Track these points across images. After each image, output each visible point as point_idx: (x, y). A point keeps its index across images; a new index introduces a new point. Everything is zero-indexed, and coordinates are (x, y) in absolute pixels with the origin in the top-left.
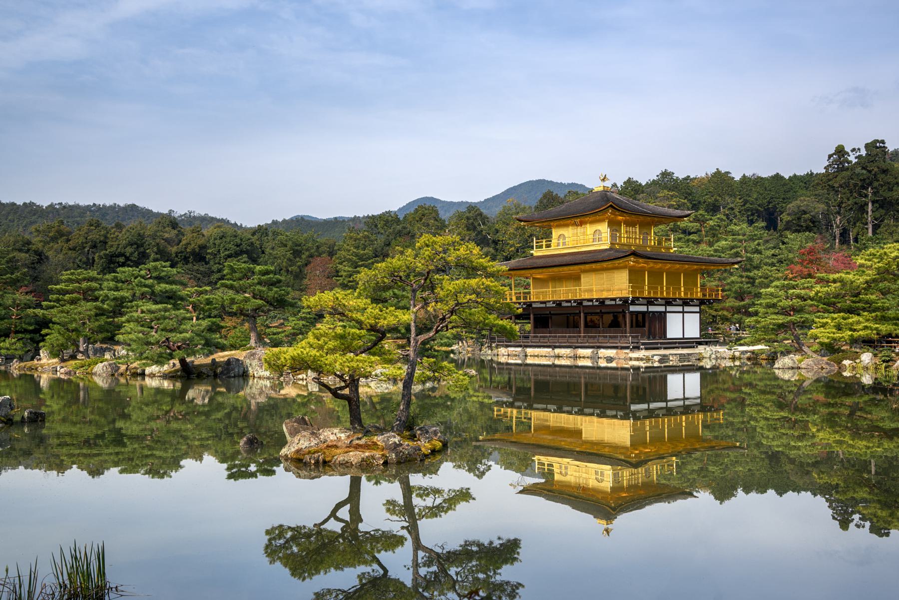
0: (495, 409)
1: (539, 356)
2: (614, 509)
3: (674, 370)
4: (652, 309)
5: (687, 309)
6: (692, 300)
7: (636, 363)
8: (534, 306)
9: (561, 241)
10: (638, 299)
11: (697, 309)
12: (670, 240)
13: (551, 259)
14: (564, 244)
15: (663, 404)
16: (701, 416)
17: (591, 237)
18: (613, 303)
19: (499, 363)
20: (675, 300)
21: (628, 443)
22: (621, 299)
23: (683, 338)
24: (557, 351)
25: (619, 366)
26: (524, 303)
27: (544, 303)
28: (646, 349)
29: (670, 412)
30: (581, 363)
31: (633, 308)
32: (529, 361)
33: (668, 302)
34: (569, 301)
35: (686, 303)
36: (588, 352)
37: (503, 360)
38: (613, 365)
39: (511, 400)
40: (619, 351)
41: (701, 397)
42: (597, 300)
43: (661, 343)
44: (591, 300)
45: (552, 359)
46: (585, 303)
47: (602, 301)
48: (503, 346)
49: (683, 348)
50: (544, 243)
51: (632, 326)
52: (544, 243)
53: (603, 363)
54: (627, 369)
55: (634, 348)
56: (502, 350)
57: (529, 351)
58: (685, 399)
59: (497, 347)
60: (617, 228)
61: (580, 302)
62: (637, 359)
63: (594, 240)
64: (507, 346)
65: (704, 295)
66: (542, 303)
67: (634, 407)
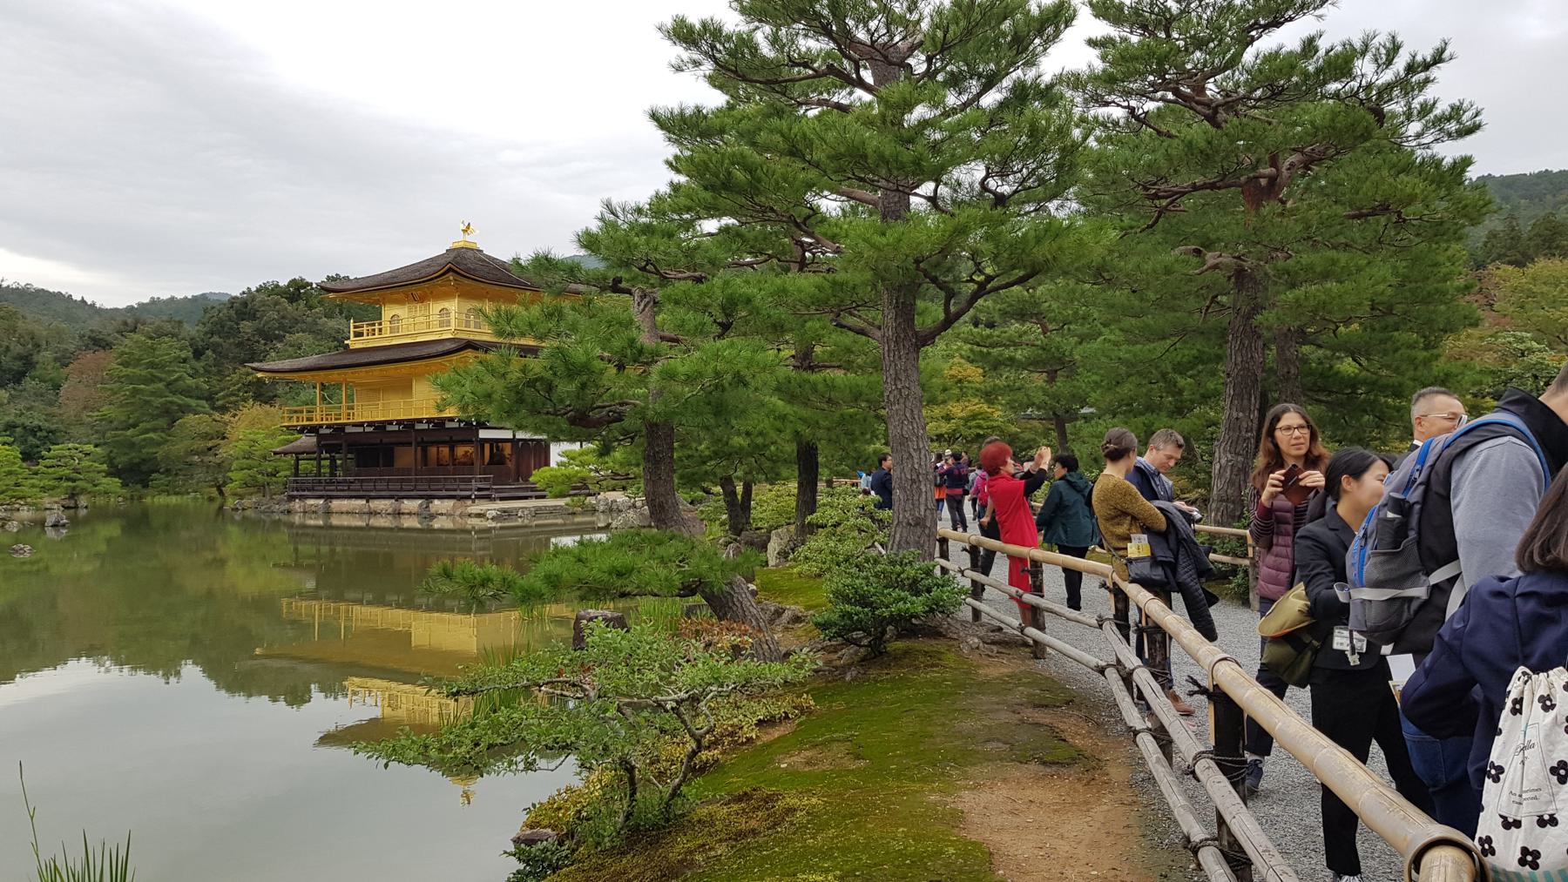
8: (349, 430)
24: (377, 504)
25: (458, 526)
27: (361, 425)
30: (412, 522)
31: (483, 434)
32: (335, 521)
34: (390, 422)
37: (297, 519)
40: (459, 503)
44: (420, 421)
46: (419, 427)
56: (297, 504)
57: (335, 504)
59: (292, 498)
64: (302, 498)
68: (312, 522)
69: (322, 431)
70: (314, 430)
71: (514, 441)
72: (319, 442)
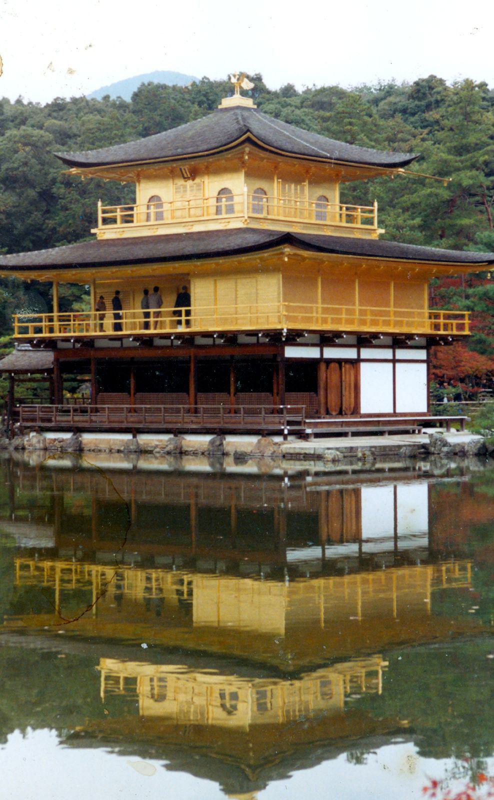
0: (18, 562)
1: (106, 449)
2: (253, 768)
3: (376, 477)
4: (331, 353)
5: (401, 354)
6: (410, 336)
9: (153, 210)
10: (299, 333)
11: (422, 354)
12: (372, 211)
13: (112, 249)
14: (159, 216)
15: (351, 549)
16: (430, 570)
17: (213, 202)
18: (253, 340)
19: (26, 466)
20: (375, 335)
21: (283, 631)
22: (267, 333)
23: (395, 414)
25: (263, 470)
26: (78, 340)
29: (366, 563)
31: (291, 352)
33: (364, 340)
34: (166, 336)
35: (399, 341)
36: (204, 440)
38: (250, 468)
39: (50, 544)
41: (431, 533)
42: (222, 334)
43: (348, 424)
45: (133, 456)
47: (230, 338)
48: (32, 429)
49: (391, 433)
50: (119, 214)
52: (119, 214)
53: (231, 468)
54: (280, 478)
55: (291, 433)
57: (88, 438)
58: (396, 538)
59: (23, 431)
60: (264, 185)
61: (188, 339)
63: (218, 211)
65: (437, 327)
67: (294, 555)
68: (51, 463)
69: (61, 345)
70: (50, 344)
71: (321, 359)
72: (57, 360)
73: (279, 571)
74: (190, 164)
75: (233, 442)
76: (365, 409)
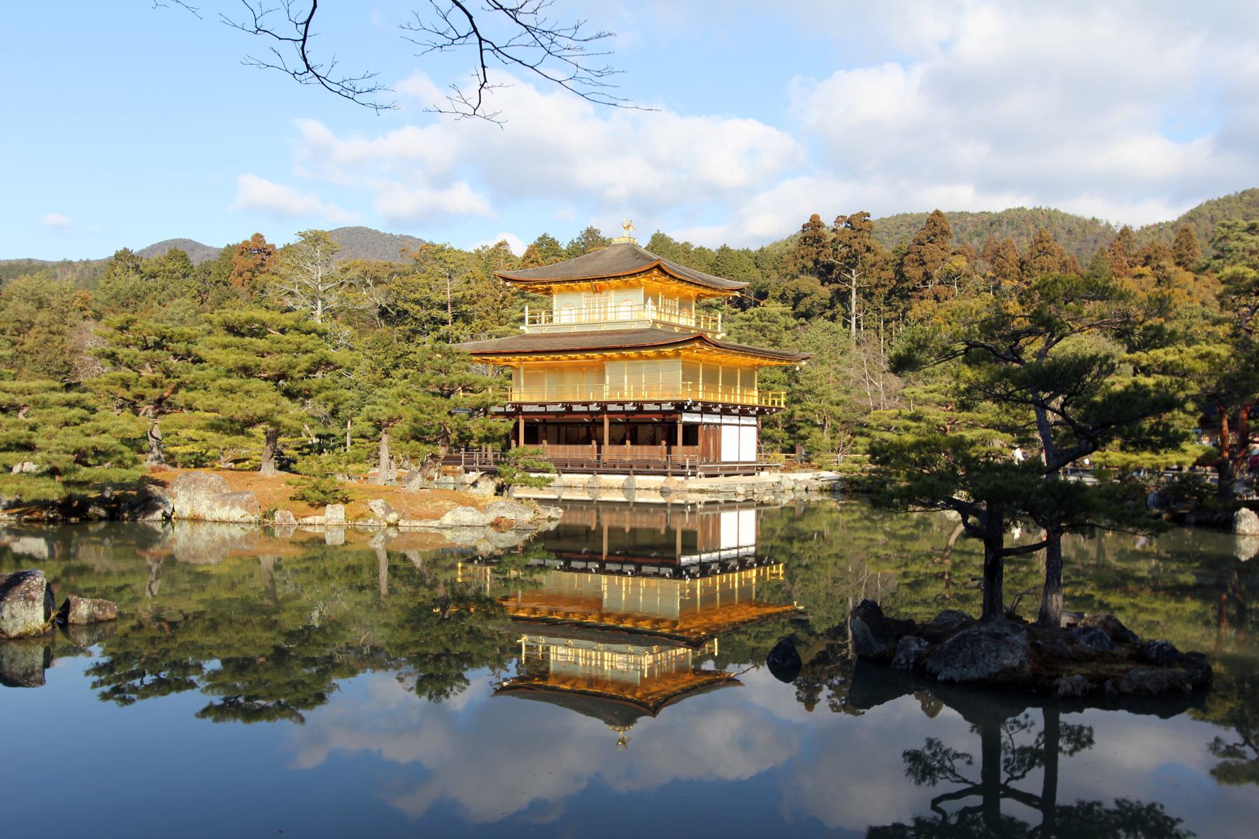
5: (744, 420)
7: (693, 498)
11: (753, 421)
15: (715, 555)
28: (707, 476)
29: (724, 566)
31: (687, 418)
33: (726, 411)
35: (744, 412)
43: (722, 469)
46: (611, 408)
47: (639, 405)
51: (685, 443)
58: (738, 548)
61: (603, 406)
62: (702, 491)
66: (541, 405)
67: (684, 560)
73: (679, 573)
74: (597, 281)
75: (640, 480)
76: (724, 459)
